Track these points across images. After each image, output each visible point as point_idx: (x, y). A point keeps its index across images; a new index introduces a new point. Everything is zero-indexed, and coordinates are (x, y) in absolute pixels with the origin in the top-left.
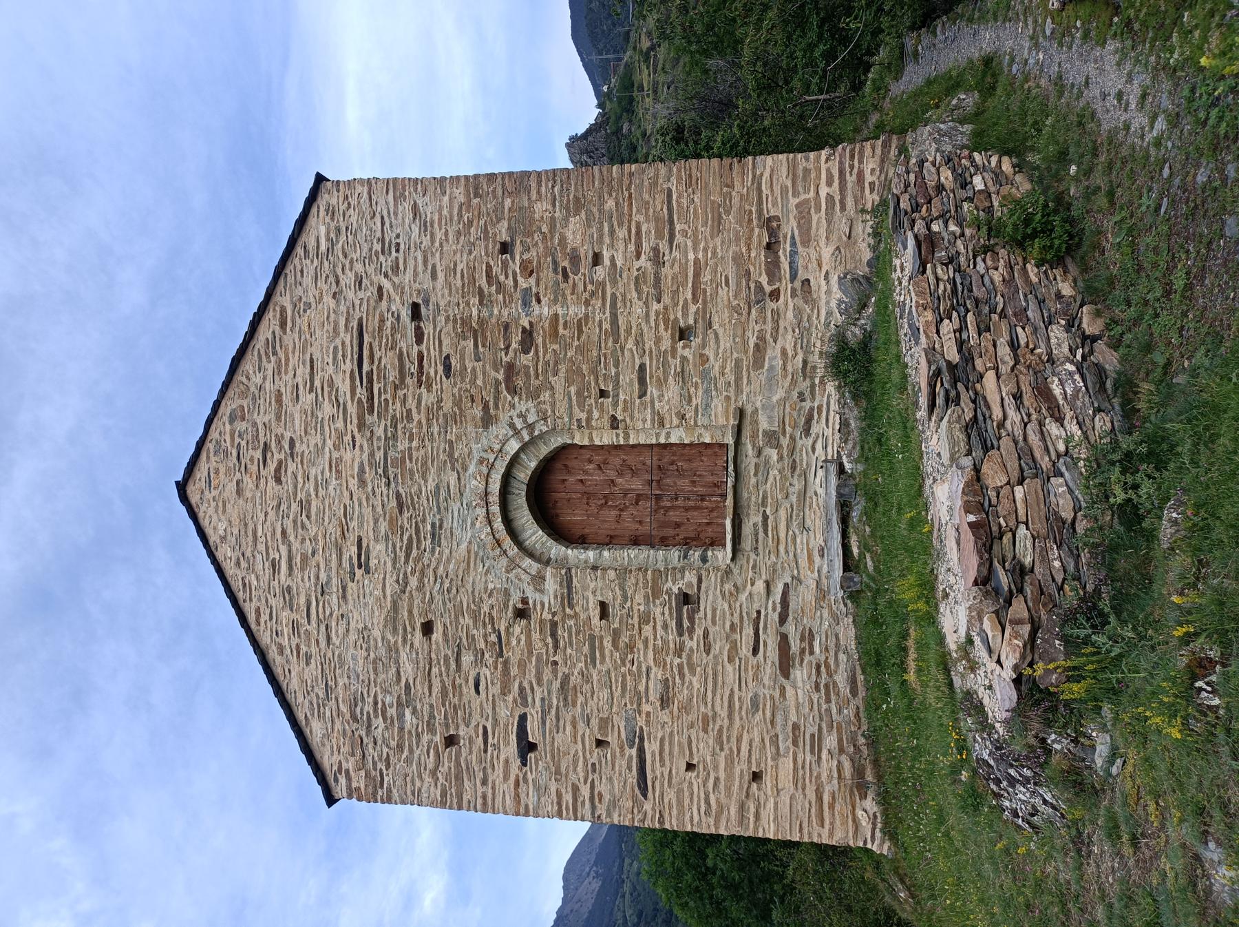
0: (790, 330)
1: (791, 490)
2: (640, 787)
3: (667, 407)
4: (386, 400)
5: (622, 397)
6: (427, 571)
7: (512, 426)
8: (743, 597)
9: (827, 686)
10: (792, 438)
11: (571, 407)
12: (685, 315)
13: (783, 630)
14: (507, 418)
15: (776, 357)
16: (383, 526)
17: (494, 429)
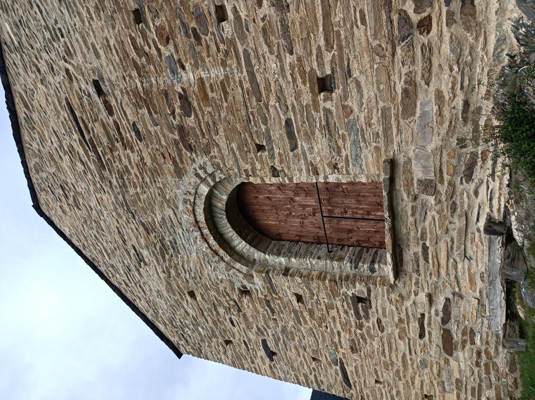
0: (446, 68)
1: (451, 227)
2: (346, 383)
3: (318, 159)
4: (109, 159)
5: (276, 151)
6: (178, 267)
7: (197, 175)
8: (408, 303)
9: (486, 365)
10: (452, 184)
11: (236, 160)
12: (321, 65)
13: (447, 327)
14: (192, 170)
15: (429, 102)
16: (142, 241)
17: (186, 179)
